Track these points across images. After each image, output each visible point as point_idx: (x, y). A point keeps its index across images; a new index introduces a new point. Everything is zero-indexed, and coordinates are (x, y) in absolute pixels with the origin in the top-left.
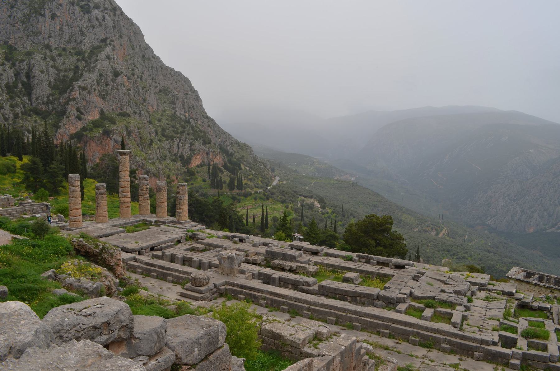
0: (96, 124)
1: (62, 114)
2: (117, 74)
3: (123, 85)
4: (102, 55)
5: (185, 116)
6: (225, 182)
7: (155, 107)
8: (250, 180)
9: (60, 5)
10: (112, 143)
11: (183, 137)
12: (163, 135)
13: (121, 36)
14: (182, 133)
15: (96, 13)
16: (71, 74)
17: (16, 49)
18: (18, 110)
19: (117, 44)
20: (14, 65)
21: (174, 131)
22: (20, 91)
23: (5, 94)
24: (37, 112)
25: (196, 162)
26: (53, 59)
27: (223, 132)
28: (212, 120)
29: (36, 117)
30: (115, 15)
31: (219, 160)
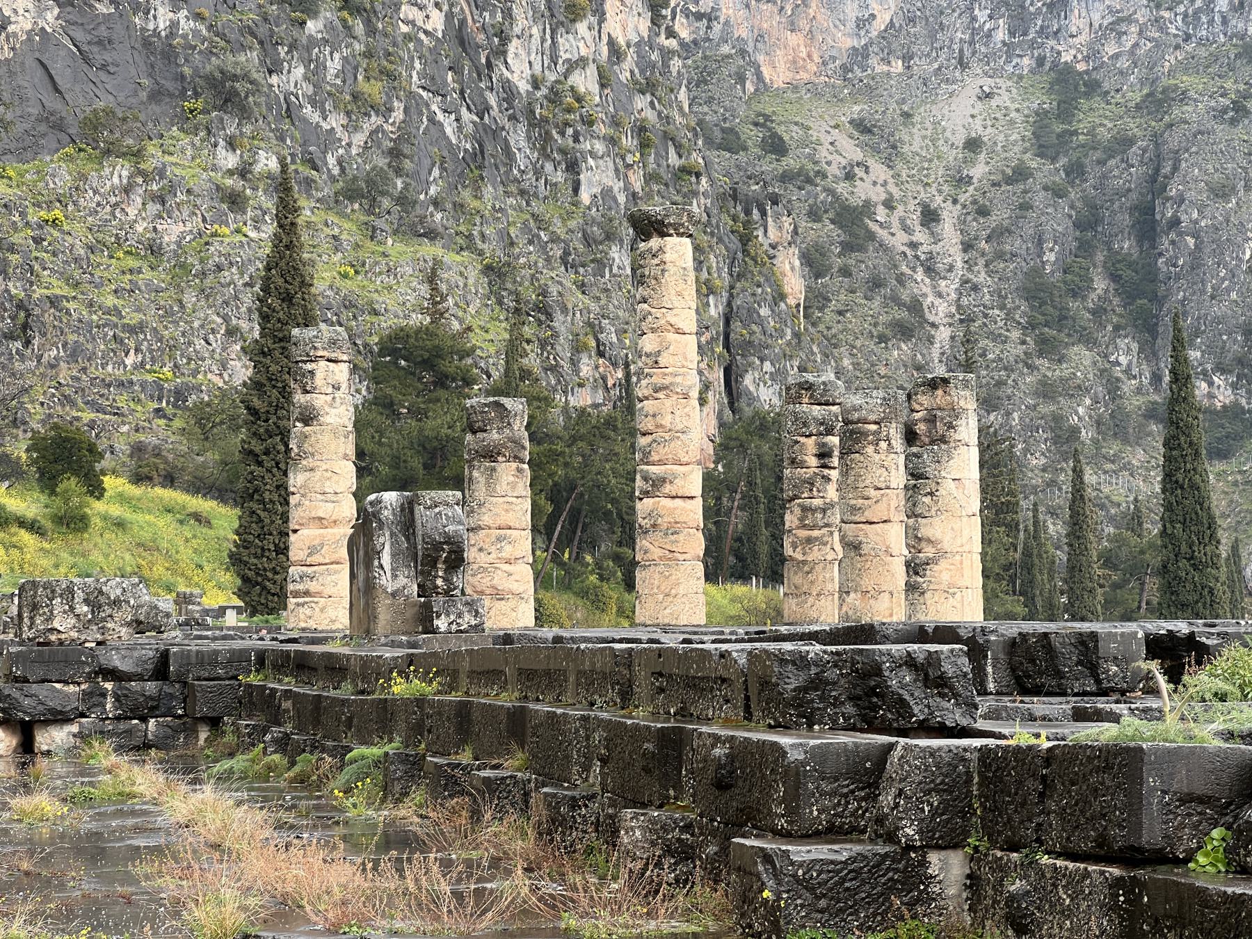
17: (1093, 87)
18: (1080, 413)
22: (1098, 312)
23: (1015, 334)
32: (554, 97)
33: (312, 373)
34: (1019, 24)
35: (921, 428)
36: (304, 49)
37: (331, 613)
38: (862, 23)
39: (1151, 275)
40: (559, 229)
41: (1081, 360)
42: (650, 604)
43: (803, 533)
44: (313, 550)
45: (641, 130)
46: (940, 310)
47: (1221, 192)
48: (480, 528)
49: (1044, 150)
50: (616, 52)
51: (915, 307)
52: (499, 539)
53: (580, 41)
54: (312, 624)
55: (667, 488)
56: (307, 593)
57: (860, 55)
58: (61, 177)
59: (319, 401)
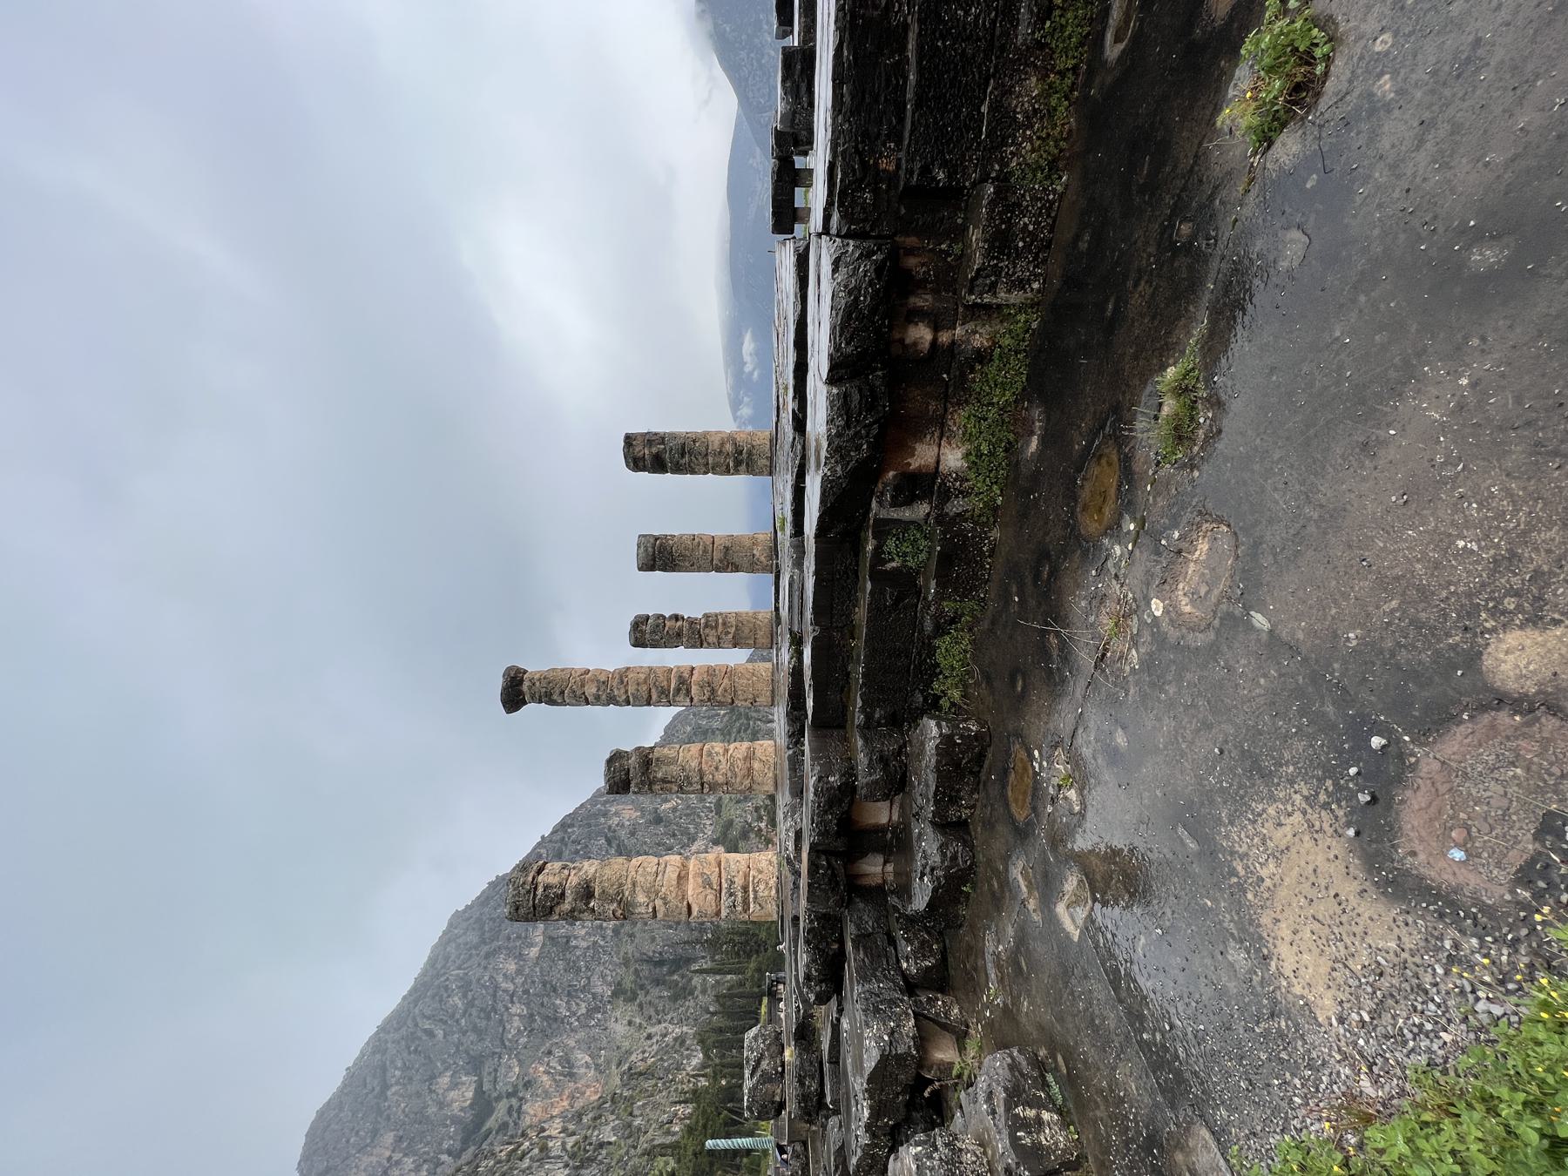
2: (658, 820)
3: (674, 809)
13: (605, 815)
14: (748, 719)
17: (619, 984)
20: (642, 987)
30: (572, 826)
32: (573, 1156)
33: (546, 888)
34: (597, 1009)
35: (654, 450)
37: (764, 864)
38: (587, 1066)
39: (674, 961)
40: (623, 1151)
41: (697, 980)
42: (759, 686)
43: (720, 628)
44: (707, 883)
45: (595, 1119)
47: (653, 939)
48: (700, 770)
50: (564, 1130)
51: (676, 1039)
52: (710, 754)
54: (773, 882)
55: (686, 675)
56: (745, 889)
57: (597, 1066)
59: (574, 880)
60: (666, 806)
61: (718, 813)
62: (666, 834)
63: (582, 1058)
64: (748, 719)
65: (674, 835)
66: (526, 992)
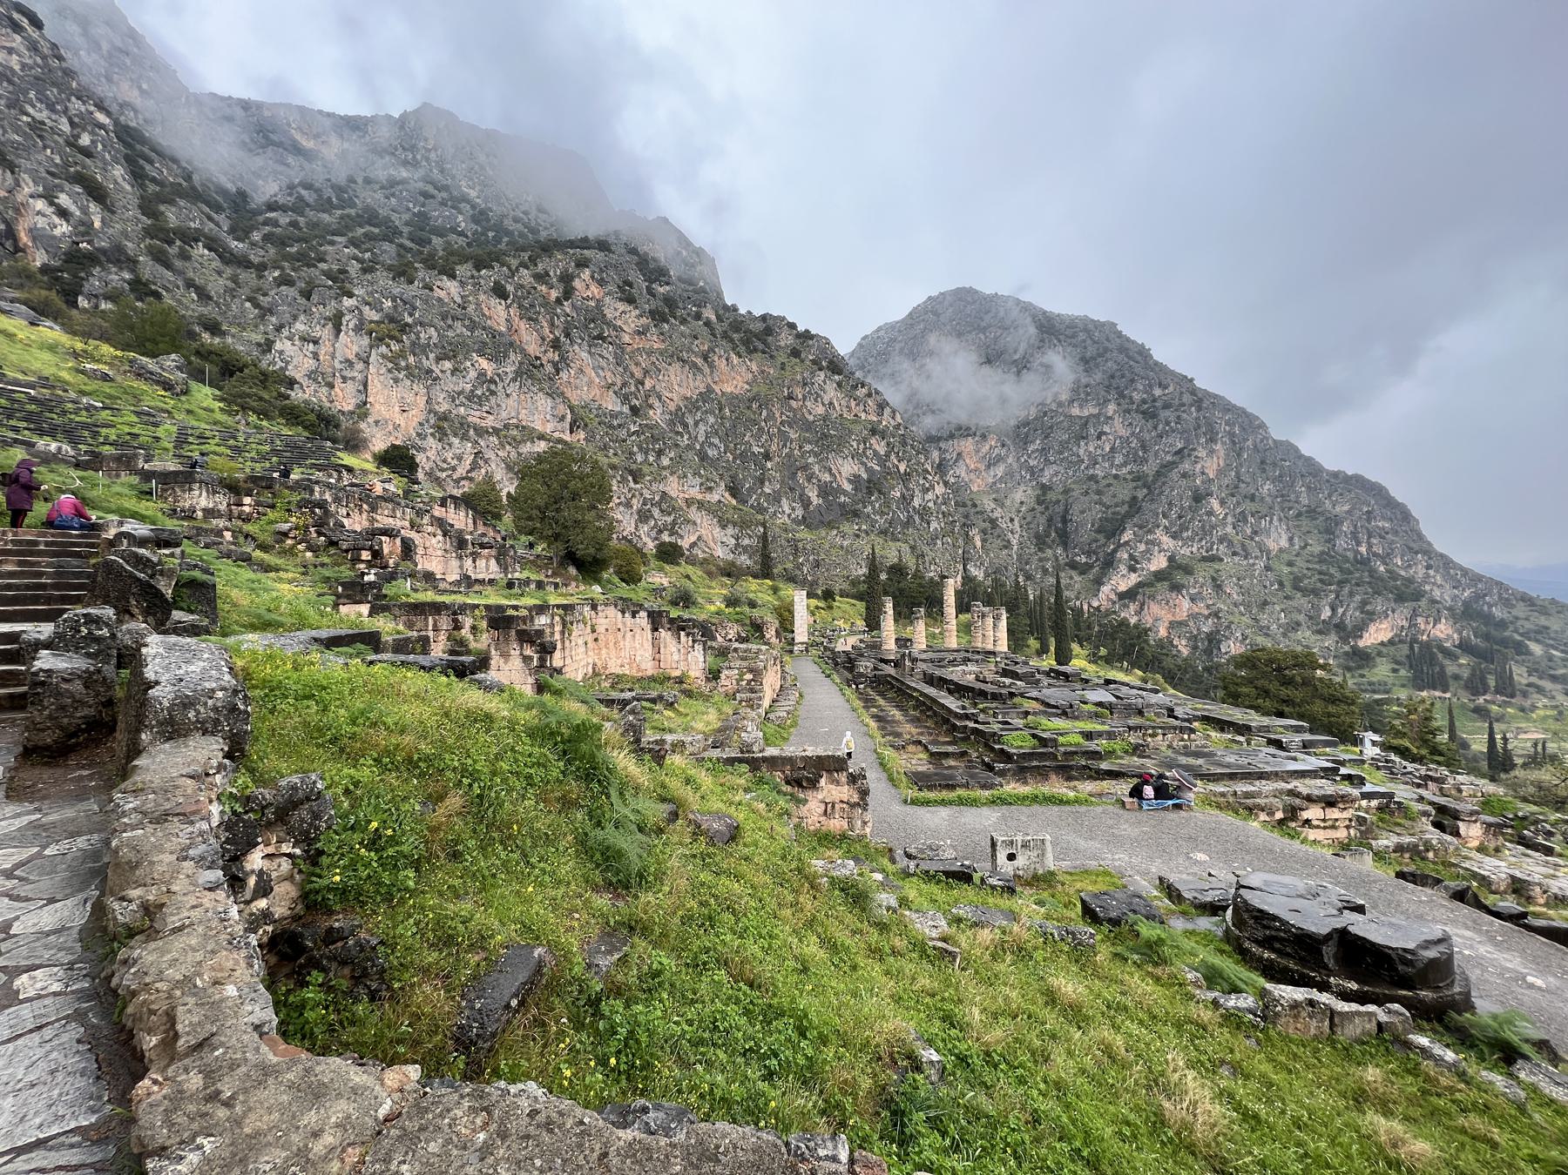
0: (1160, 576)
1: (1109, 563)
2: (1198, 498)
3: (1210, 513)
4: (1174, 475)
5: (1357, 552)
6: (1456, 677)
7: (1284, 543)
8: (1554, 678)
9: (1111, 418)
10: (1186, 604)
11: (1346, 590)
12: (1296, 588)
14: (1341, 583)
15: (1164, 414)
16: (1123, 509)
17: (1051, 488)
18: (1048, 565)
19: (1202, 453)
20: (1047, 508)
21: (1321, 581)
24: (1073, 565)
25: (1376, 635)
26: (1099, 493)
27: (1477, 578)
28: (1442, 555)
29: (1074, 573)
30: (1199, 409)
31: (1443, 631)
34: (1032, 474)
36: (871, 503)
41: (1049, 552)
46: (1014, 542)
47: (1082, 512)
49: (1039, 504)
53: (930, 496)
58: (823, 533)
60: (1215, 504)
61: (1204, 559)
62: (1182, 508)
63: (1000, 470)
64: (1341, 583)
65: (1180, 517)
66: (1045, 414)
